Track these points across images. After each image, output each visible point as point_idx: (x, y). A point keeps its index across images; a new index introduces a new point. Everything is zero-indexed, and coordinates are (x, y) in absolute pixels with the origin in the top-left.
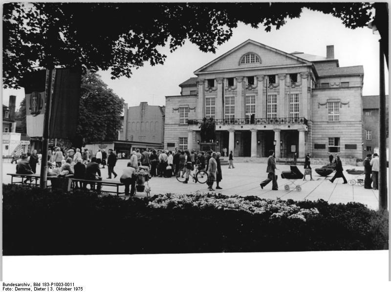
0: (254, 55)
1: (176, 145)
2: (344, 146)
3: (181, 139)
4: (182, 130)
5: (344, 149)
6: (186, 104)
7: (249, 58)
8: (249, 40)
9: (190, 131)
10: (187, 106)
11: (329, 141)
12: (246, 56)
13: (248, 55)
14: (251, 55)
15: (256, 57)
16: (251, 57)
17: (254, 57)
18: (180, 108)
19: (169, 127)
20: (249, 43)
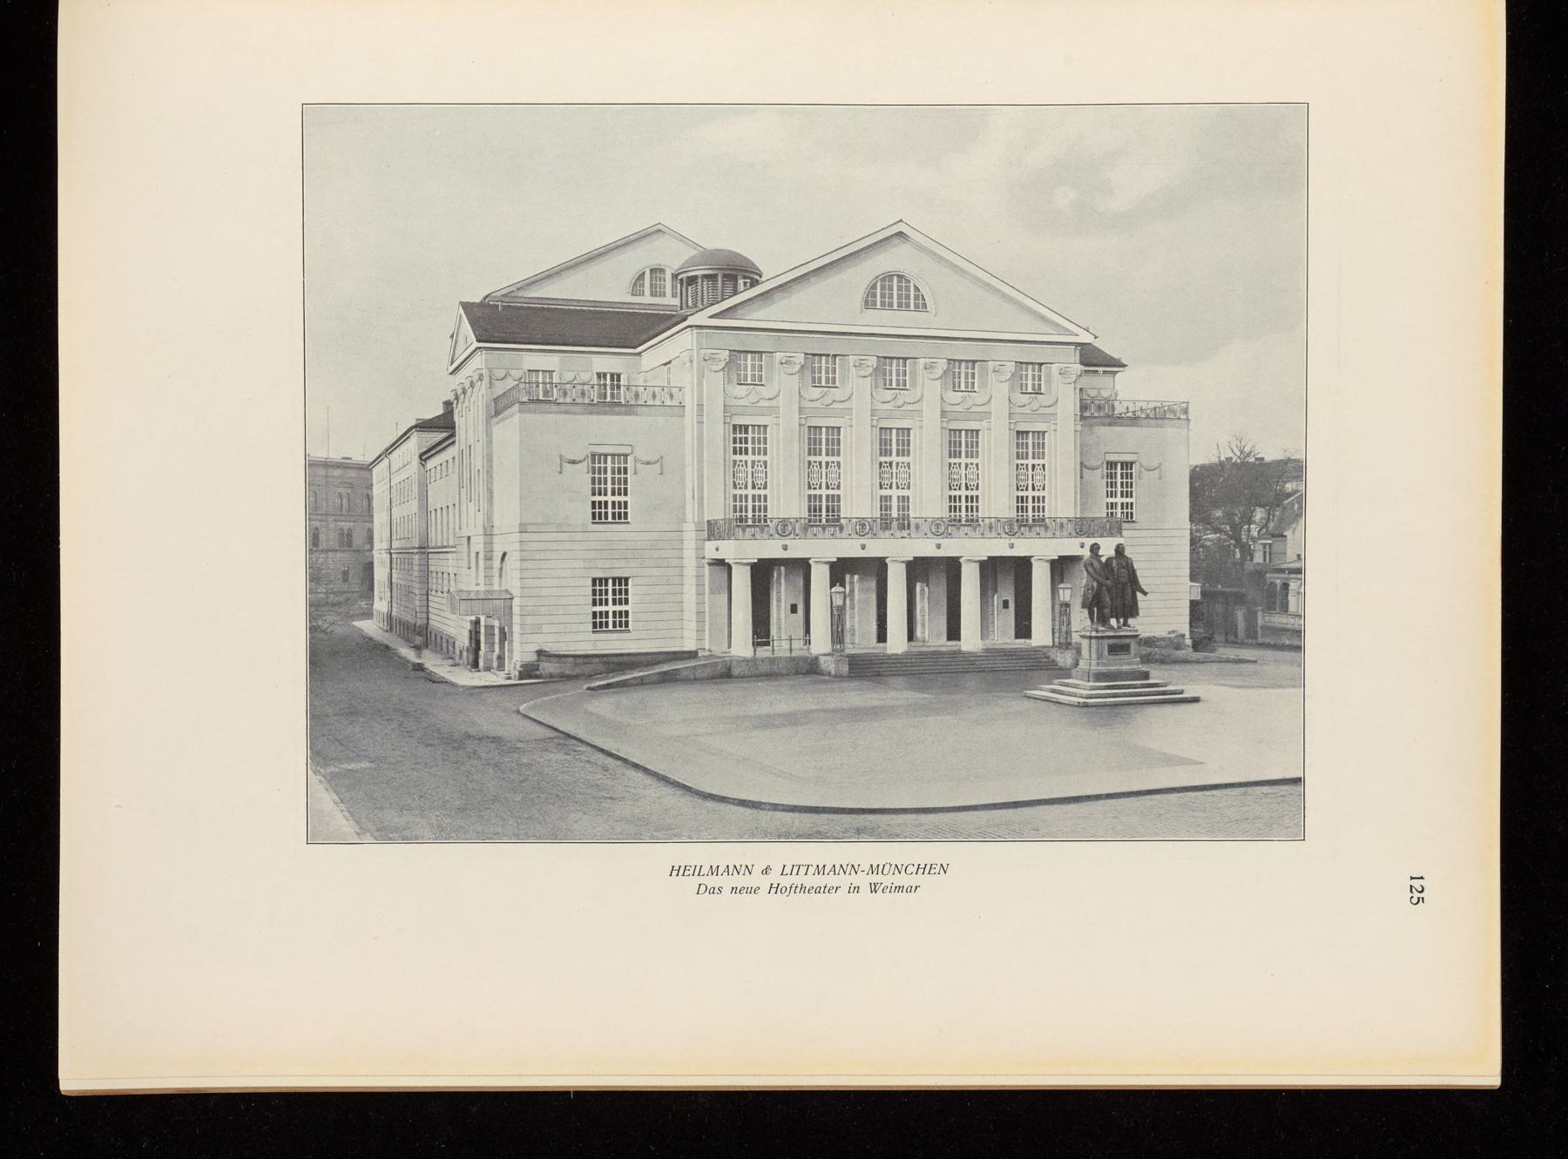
7: (891, 289)
13: (887, 277)
15: (915, 286)
16: (900, 288)
17: (908, 289)
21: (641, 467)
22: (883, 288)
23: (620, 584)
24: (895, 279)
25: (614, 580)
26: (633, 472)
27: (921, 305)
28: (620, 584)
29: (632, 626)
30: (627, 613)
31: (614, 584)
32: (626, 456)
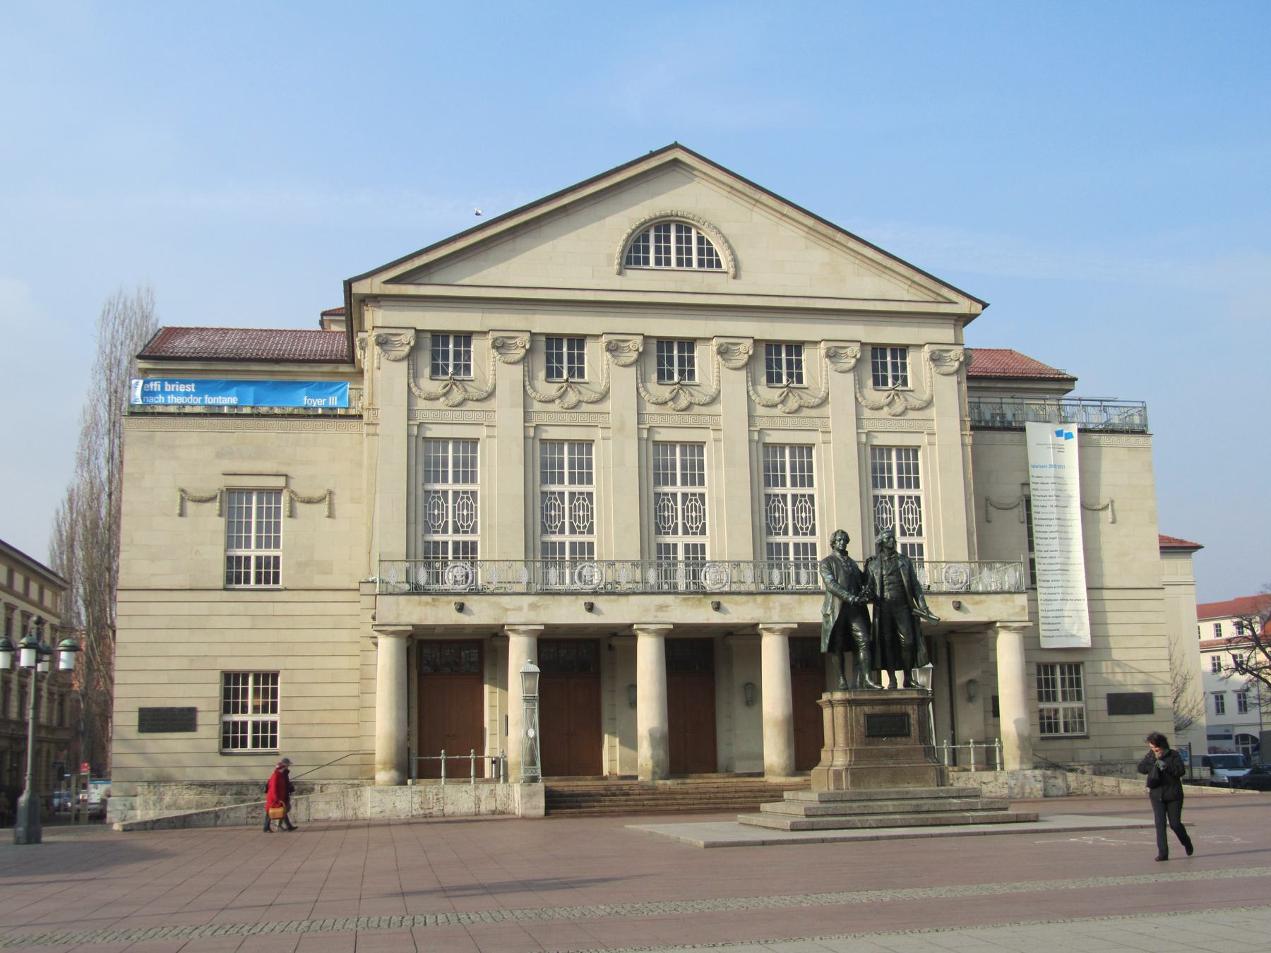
0: (689, 230)
1: (201, 719)
2: (1103, 704)
3: (232, 682)
4: (246, 622)
5: (1104, 716)
6: (268, 467)
7: (668, 240)
8: (675, 146)
9: (382, 629)
10: (280, 482)
11: (1039, 681)
12: (658, 229)
13: (661, 225)
14: (679, 229)
15: (701, 240)
16: (679, 240)
18: (231, 491)
19: (154, 609)
20: (676, 162)
21: (300, 507)
22: (658, 239)
23: (266, 683)
24: (673, 229)
25: (257, 676)
26: (287, 513)
27: (709, 260)
28: (266, 683)
29: (281, 746)
30: (274, 724)
31: (256, 682)
32: (278, 492)
